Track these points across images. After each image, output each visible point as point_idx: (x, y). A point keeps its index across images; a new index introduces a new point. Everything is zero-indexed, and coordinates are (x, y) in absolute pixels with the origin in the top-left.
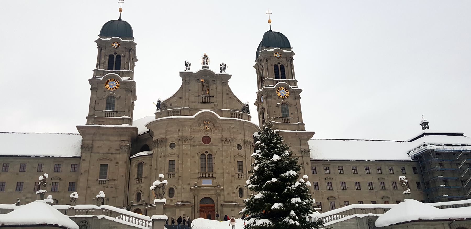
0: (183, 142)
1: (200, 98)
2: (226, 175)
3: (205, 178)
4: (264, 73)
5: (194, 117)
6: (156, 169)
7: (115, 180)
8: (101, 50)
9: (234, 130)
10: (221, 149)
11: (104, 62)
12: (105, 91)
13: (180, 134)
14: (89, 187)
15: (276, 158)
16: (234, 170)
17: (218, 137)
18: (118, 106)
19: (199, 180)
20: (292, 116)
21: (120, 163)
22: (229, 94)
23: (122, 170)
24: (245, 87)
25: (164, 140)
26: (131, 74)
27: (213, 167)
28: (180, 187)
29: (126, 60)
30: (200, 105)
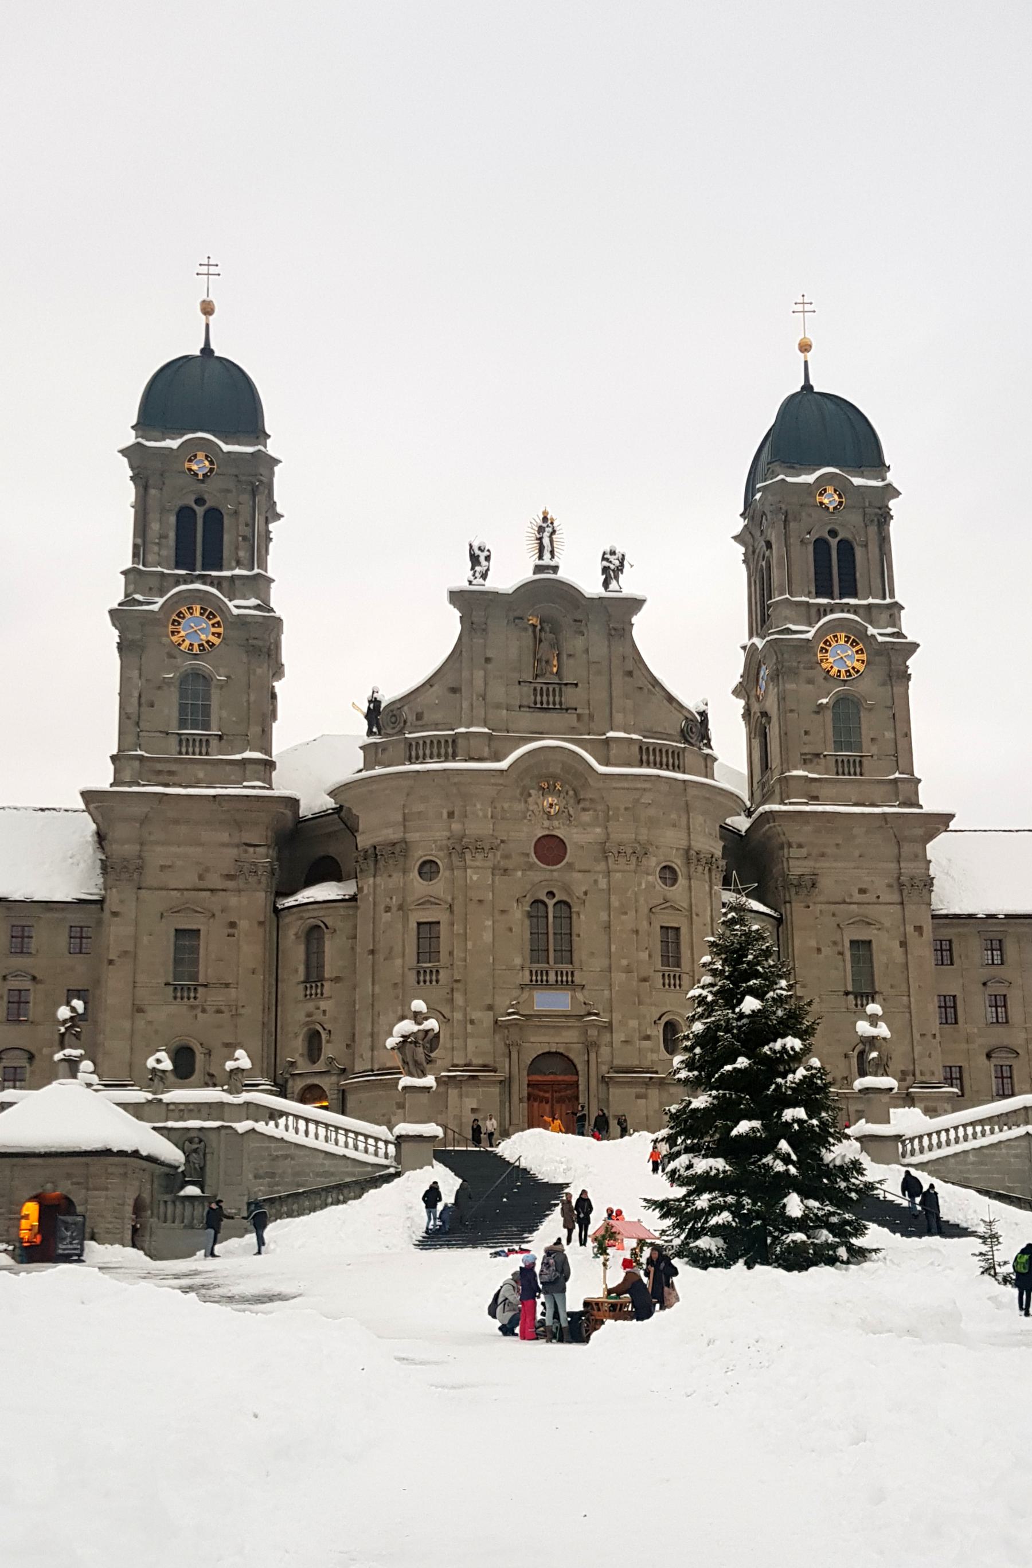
0: (468, 856)
1: (527, 690)
2: (619, 977)
3: (547, 985)
4: (775, 572)
5: (504, 765)
6: (372, 952)
7: (227, 985)
8: (146, 488)
9: (652, 812)
10: (603, 883)
11: (161, 537)
12: (171, 656)
13: (456, 827)
14: (140, 1010)
15: (750, 1004)
16: (647, 956)
18: (224, 714)
19: (526, 995)
20: (874, 750)
21: (244, 924)
22: (636, 673)
23: (251, 950)
24: (696, 636)
26: (260, 585)
27: (575, 946)
28: (458, 1016)
29: (244, 530)
30: (527, 719)
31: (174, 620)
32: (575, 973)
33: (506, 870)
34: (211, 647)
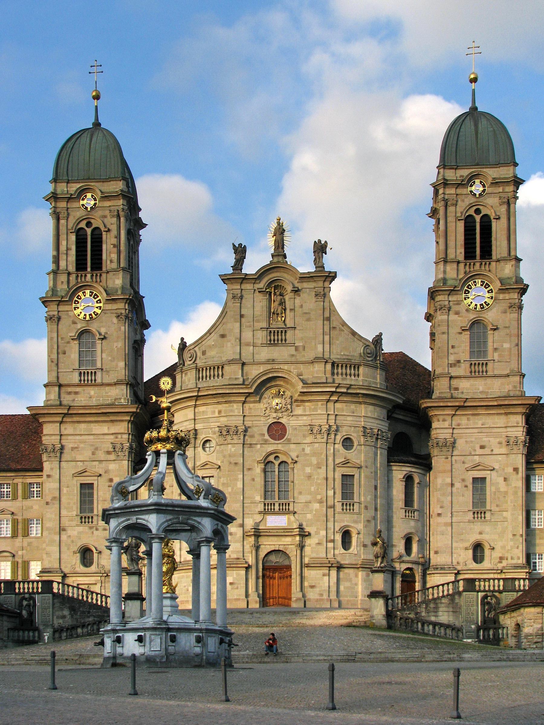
12: (74, 323)
17: (301, 423)
20: (496, 356)
25: (191, 433)
31: (76, 301)
32: (291, 504)
33: (251, 444)
34: (96, 315)
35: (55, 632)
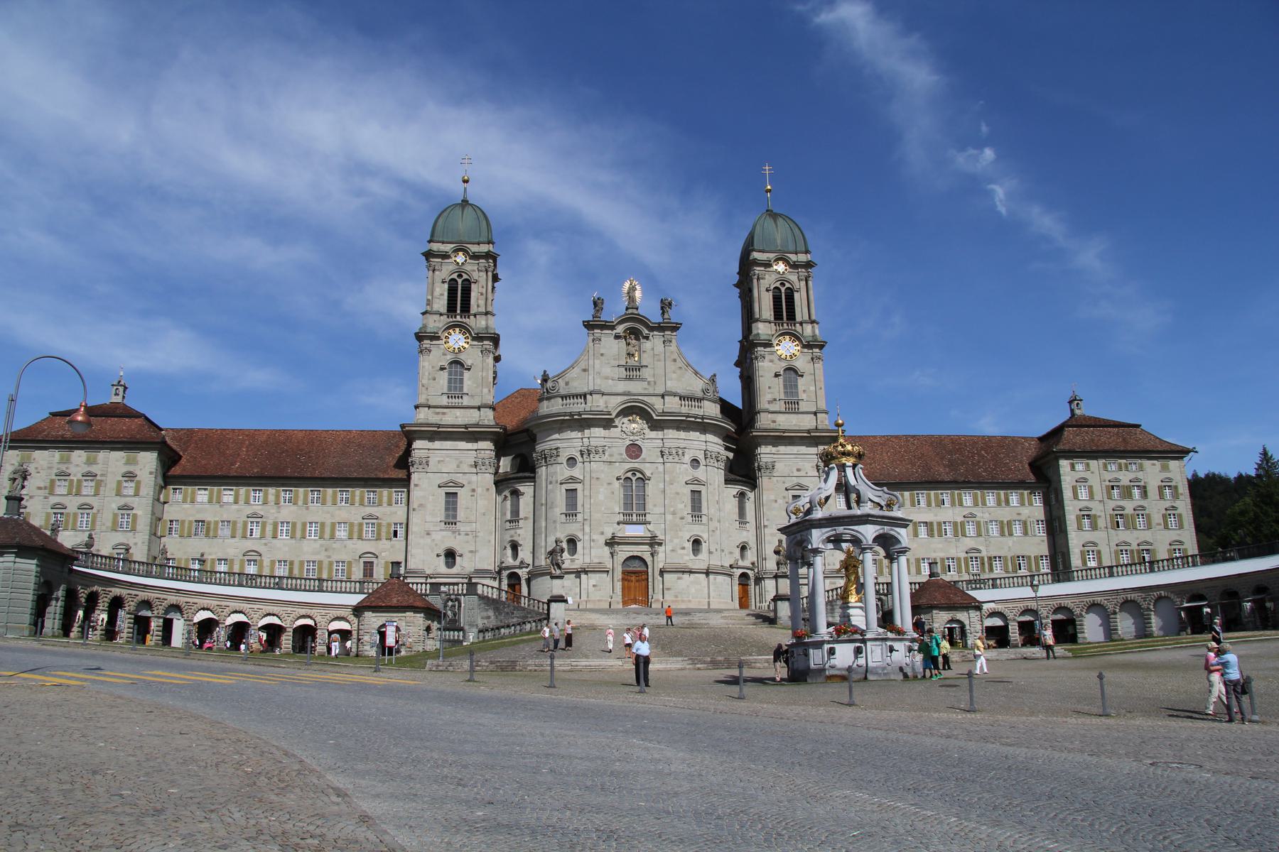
2: (669, 517)
16: (685, 507)
21: (479, 490)
28: (587, 537)
35: (480, 631)
